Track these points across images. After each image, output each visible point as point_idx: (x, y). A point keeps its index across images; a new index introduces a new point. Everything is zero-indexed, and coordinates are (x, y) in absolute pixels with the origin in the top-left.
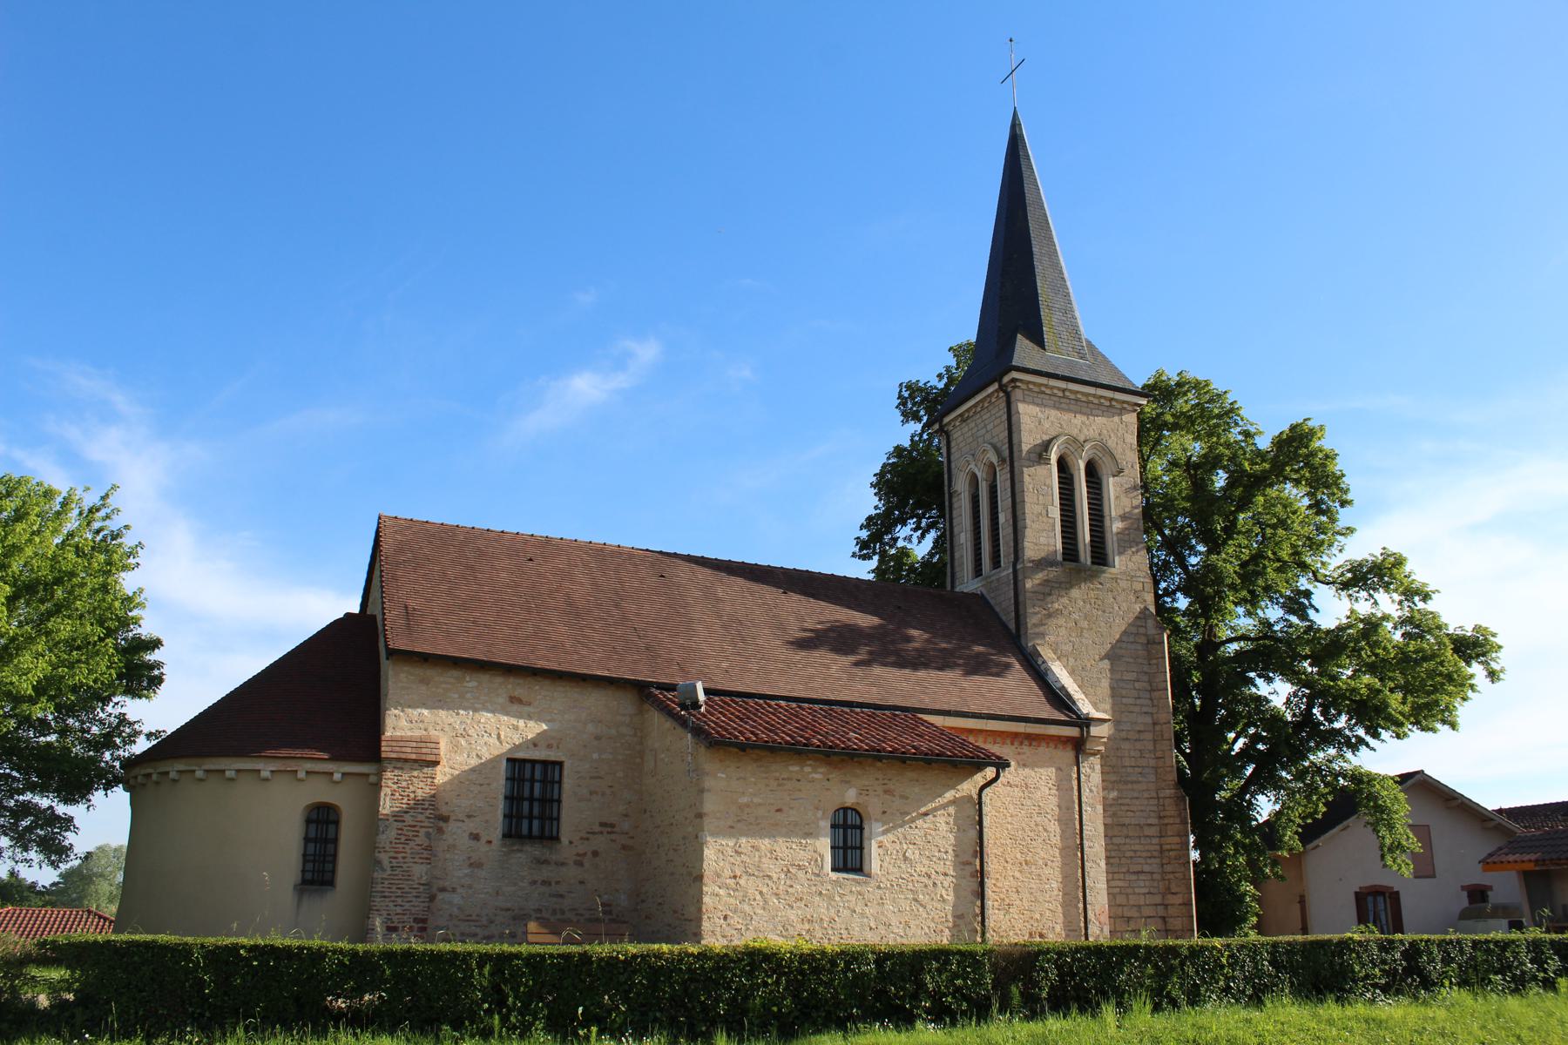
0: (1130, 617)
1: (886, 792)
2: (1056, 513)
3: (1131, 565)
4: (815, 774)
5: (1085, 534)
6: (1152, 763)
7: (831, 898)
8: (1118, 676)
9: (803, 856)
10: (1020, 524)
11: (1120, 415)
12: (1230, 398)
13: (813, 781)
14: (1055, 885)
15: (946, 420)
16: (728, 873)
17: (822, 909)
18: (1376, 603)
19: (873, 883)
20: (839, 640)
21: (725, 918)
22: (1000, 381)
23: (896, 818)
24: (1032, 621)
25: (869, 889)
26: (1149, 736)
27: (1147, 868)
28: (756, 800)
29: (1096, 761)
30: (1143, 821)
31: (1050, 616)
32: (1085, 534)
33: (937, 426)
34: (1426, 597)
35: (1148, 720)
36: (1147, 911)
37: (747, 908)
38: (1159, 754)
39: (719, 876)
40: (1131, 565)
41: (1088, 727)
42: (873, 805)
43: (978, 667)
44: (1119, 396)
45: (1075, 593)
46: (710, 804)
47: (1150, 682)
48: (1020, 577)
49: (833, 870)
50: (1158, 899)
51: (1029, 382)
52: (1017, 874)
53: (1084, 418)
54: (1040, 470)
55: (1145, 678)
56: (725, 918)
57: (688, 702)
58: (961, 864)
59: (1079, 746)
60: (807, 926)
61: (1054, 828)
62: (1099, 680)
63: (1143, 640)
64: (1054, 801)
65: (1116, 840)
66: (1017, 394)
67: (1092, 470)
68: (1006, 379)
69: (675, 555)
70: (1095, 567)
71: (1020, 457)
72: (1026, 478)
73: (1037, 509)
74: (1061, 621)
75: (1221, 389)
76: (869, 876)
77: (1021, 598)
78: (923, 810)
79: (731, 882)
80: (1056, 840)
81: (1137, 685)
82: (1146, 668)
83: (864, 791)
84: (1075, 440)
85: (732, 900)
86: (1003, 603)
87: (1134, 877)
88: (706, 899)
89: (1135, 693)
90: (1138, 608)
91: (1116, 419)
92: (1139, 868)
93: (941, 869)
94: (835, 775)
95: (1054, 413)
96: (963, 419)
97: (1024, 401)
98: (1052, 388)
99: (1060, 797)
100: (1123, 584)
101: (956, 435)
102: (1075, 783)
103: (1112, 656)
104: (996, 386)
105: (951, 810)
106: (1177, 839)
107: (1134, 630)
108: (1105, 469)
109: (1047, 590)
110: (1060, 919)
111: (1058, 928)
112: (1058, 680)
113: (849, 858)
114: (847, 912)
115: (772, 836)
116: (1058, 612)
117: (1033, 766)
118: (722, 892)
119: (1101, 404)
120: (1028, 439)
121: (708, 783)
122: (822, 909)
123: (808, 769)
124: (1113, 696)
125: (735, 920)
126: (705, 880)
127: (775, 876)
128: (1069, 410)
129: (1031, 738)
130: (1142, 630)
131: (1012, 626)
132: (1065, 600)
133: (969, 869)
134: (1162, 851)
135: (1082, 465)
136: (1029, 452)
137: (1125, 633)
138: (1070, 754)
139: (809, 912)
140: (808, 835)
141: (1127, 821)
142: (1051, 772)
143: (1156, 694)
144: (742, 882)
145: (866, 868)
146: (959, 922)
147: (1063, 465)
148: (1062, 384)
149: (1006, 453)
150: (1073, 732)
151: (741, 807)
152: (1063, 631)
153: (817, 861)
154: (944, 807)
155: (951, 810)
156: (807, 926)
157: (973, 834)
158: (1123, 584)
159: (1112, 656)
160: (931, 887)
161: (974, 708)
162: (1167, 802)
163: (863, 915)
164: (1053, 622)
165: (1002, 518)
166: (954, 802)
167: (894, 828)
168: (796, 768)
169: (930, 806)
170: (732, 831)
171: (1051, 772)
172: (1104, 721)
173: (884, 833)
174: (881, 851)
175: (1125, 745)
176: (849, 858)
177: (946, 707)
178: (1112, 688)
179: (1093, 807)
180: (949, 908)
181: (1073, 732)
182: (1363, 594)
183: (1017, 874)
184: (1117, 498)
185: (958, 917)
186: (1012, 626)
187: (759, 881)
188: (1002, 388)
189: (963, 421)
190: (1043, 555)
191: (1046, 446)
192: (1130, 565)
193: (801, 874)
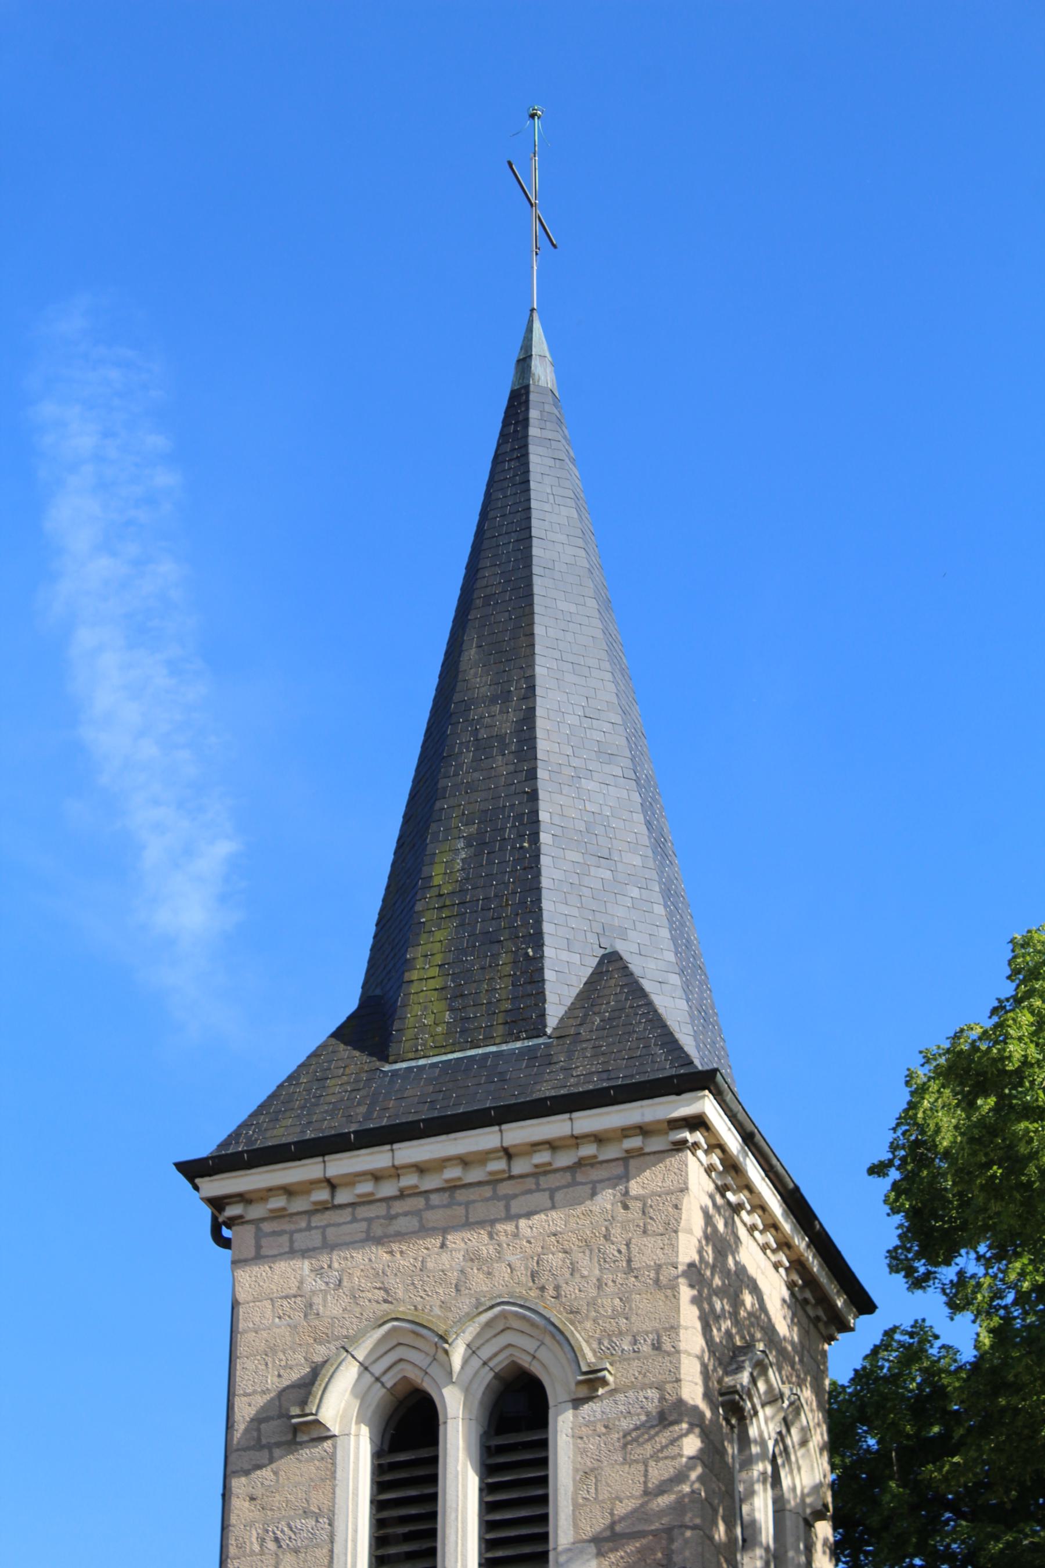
44: (588, 1121)
53: (478, 1240)
54: (296, 1468)
67: (517, 1414)
91: (607, 1199)
95: (360, 1263)
108: (558, 1387)
128: (424, 1230)
136: (258, 1420)
147: (408, 1429)
148: (377, 1158)
184: (587, 1474)
191: (308, 1386)
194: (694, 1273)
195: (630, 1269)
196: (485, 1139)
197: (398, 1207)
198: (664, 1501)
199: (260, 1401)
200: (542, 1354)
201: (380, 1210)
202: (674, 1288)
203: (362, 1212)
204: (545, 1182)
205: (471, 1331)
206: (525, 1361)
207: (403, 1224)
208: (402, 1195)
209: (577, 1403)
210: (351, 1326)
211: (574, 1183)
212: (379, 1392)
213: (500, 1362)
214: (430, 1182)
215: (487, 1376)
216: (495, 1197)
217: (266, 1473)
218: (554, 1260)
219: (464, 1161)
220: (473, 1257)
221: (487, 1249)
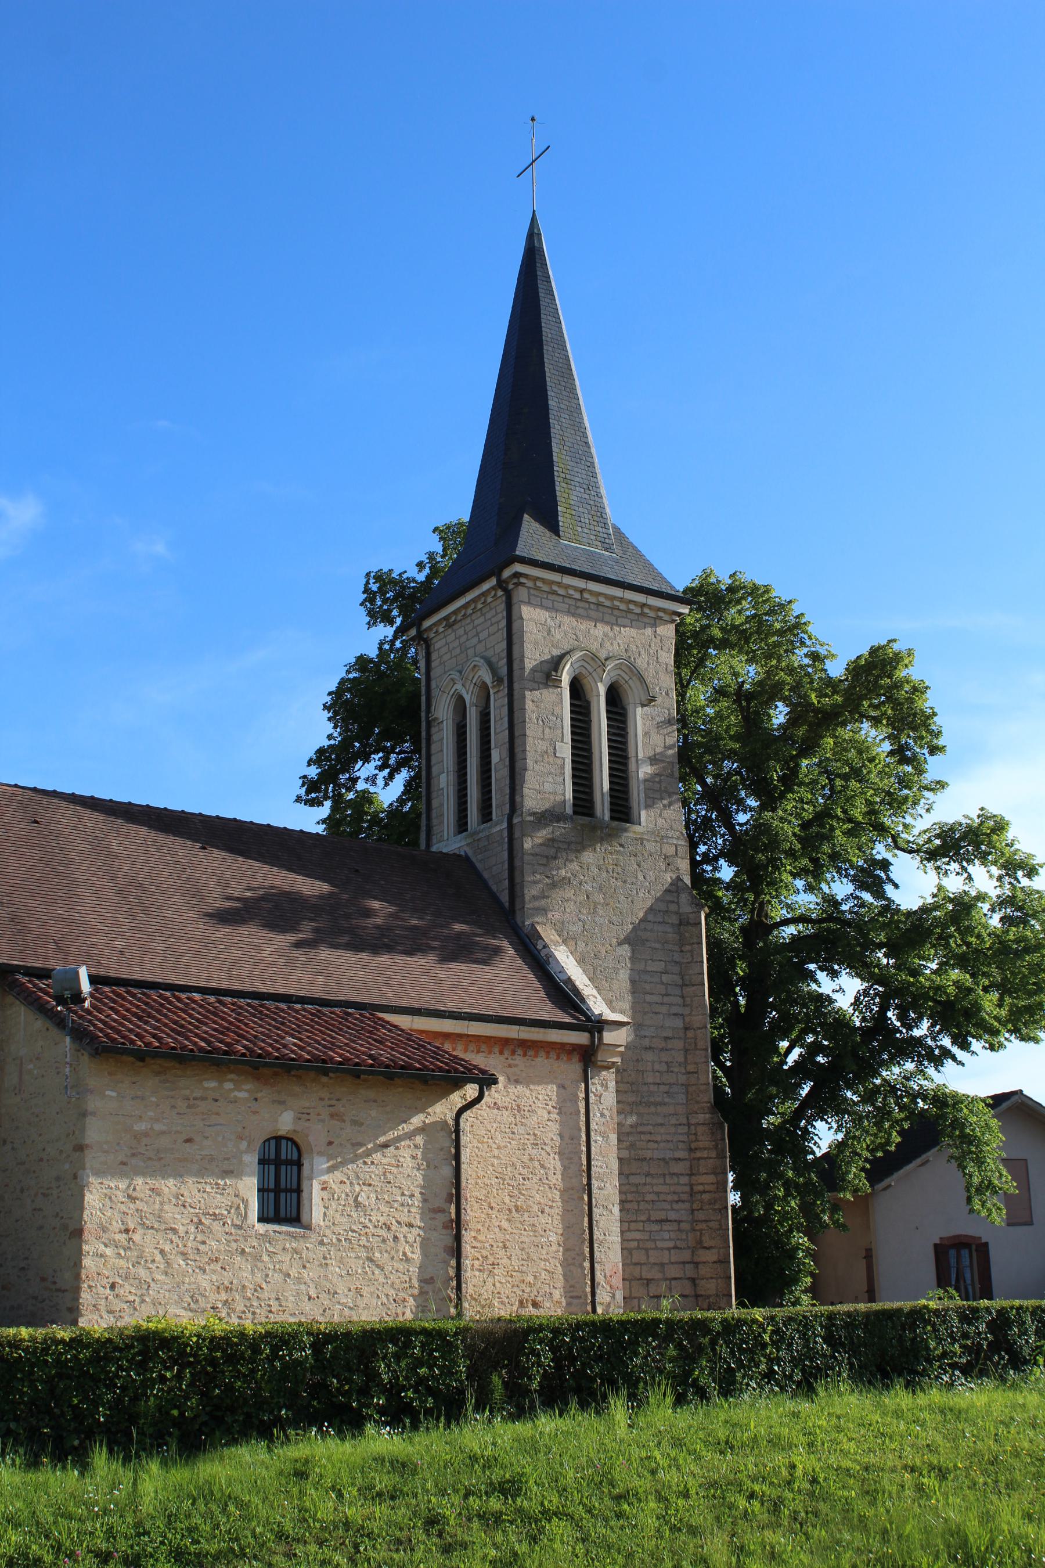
0: (659, 890)
1: (332, 1116)
2: (565, 751)
3: (661, 822)
4: (239, 1090)
6: (682, 1079)
7: (257, 1258)
8: (642, 967)
9: (220, 1202)
10: (518, 765)
11: (654, 625)
12: (796, 609)
13: (235, 1101)
14: (553, 1238)
15: (427, 624)
16: (117, 1226)
17: (244, 1273)
18: (970, 878)
19: (314, 1237)
20: (274, 912)
21: (113, 1287)
22: (499, 575)
23: (347, 1151)
24: (530, 892)
25: (309, 1245)
26: (679, 1044)
27: (672, 1216)
28: (158, 1127)
29: (609, 1077)
30: (669, 1155)
31: (554, 886)
33: (413, 632)
34: (1031, 872)
35: (679, 1023)
36: (673, 1271)
37: (143, 1273)
38: (691, 1068)
39: (104, 1230)
40: (661, 822)
41: (600, 1031)
42: (315, 1134)
43: (458, 951)
45: (588, 856)
46: (95, 1132)
47: (682, 976)
48: (517, 834)
49: (261, 1220)
50: (686, 1255)
51: (538, 578)
52: (505, 1224)
53: (607, 629)
54: (547, 695)
55: (676, 969)
56: (113, 1287)
57: (67, 994)
58: (430, 1211)
59: (588, 1057)
60: (224, 1296)
61: (554, 1163)
62: (616, 971)
63: (674, 919)
64: (555, 1127)
65: (633, 1179)
66: (521, 594)
68: (507, 573)
69: (55, 794)
70: (615, 823)
71: (522, 677)
72: (529, 705)
73: (542, 746)
74: (569, 893)
75: (785, 597)
76: (308, 1227)
77: (517, 863)
78: (382, 1140)
79: (122, 1238)
80: (556, 1179)
81: (665, 978)
82: (677, 957)
83: (303, 1115)
84: (594, 657)
85: (123, 1263)
86: (493, 867)
87: (656, 1227)
88: (87, 1262)
89: (662, 989)
90: (668, 878)
91: (649, 631)
92: (662, 1215)
93: (404, 1219)
94: (265, 1094)
95: (567, 620)
96: (449, 623)
97: (529, 603)
98: (567, 587)
99: (562, 1124)
100: (651, 846)
101: (438, 644)
102: (582, 1105)
103: (634, 940)
104: (493, 581)
105: (419, 1140)
106: (712, 1178)
107: (662, 906)
108: (632, 695)
109: (552, 852)
110: (560, 1282)
111: (557, 1294)
112: (562, 971)
113: (283, 1203)
114: (278, 1277)
115: (178, 1175)
116: (566, 881)
117: (527, 1082)
118: (108, 1251)
119: (629, 611)
120: (533, 655)
121: (93, 1103)
122: (244, 1273)
123: (228, 1085)
124: (633, 993)
125: (126, 1289)
126: (86, 1235)
127: (182, 1230)
128: (588, 618)
129: (526, 1046)
130: (673, 907)
131: (505, 898)
132: (574, 866)
133: (441, 1218)
134: (692, 1193)
135: (602, 690)
136: (533, 670)
137: (651, 910)
138: (574, 1068)
139: (227, 1277)
140: (227, 1173)
141: (649, 1154)
142: (552, 1089)
143: (689, 990)
144: (137, 1237)
145: (304, 1218)
146: (427, 1287)
148: (580, 583)
149: (504, 671)
150: (580, 1038)
151: (137, 1137)
152: (571, 907)
153: (239, 1208)
154: (410, 1136)
155: (419, 1140)
156: (224, 1296)
157: (447, 1171)
158: (651, 846)
159: (634, 940)
160: (391, 1243)
161: (452, 1006)
162: (701, 1129)
163: (299, 1280)
164: (558, 894)
165: (495, 756)
166: (422, 1130)
167: (343, 1164)
168: (213, 1084)
169: (391, 1135)
170: (124, 1168)
171: (552, 1089)
172: (620, 1024)
173: (331, 1170)
174: (325, 1195)
175: (649, 1056)
176: (283, 1203)
177: (415, 1004)
178: (633, 982)
179: (605, 1136)
180: (414, 1270)
181: (580, 1038)
182: (955, 866)
183: (505, 1224)
184: (646, 734)
185: (426, 1281)
186: (505, 898)
187: (159, 1236)
188: (501, 584)
189: (449, 626)
190: (547, 806)
191: (556, 663)
192: (660, 823)
193: (217, 1226)
195: (658, 662)
197: (579, 604)
199: (534, 663)
200: (630, 682)
201: (572, 602)
203: (566, 600)
204: (630, 616)
206: (622, 682)
207: (580, 611)
208: (582, 600)
209: (643, 705)
210: (567, 647)
211: (638, 620)
213: (613, 680)
214: (593, 599)
216: (612, 614)
217: (537, 693)
218: (633, 648)
219: (606, 596)
220: (606, 635)
221: (611, 634)
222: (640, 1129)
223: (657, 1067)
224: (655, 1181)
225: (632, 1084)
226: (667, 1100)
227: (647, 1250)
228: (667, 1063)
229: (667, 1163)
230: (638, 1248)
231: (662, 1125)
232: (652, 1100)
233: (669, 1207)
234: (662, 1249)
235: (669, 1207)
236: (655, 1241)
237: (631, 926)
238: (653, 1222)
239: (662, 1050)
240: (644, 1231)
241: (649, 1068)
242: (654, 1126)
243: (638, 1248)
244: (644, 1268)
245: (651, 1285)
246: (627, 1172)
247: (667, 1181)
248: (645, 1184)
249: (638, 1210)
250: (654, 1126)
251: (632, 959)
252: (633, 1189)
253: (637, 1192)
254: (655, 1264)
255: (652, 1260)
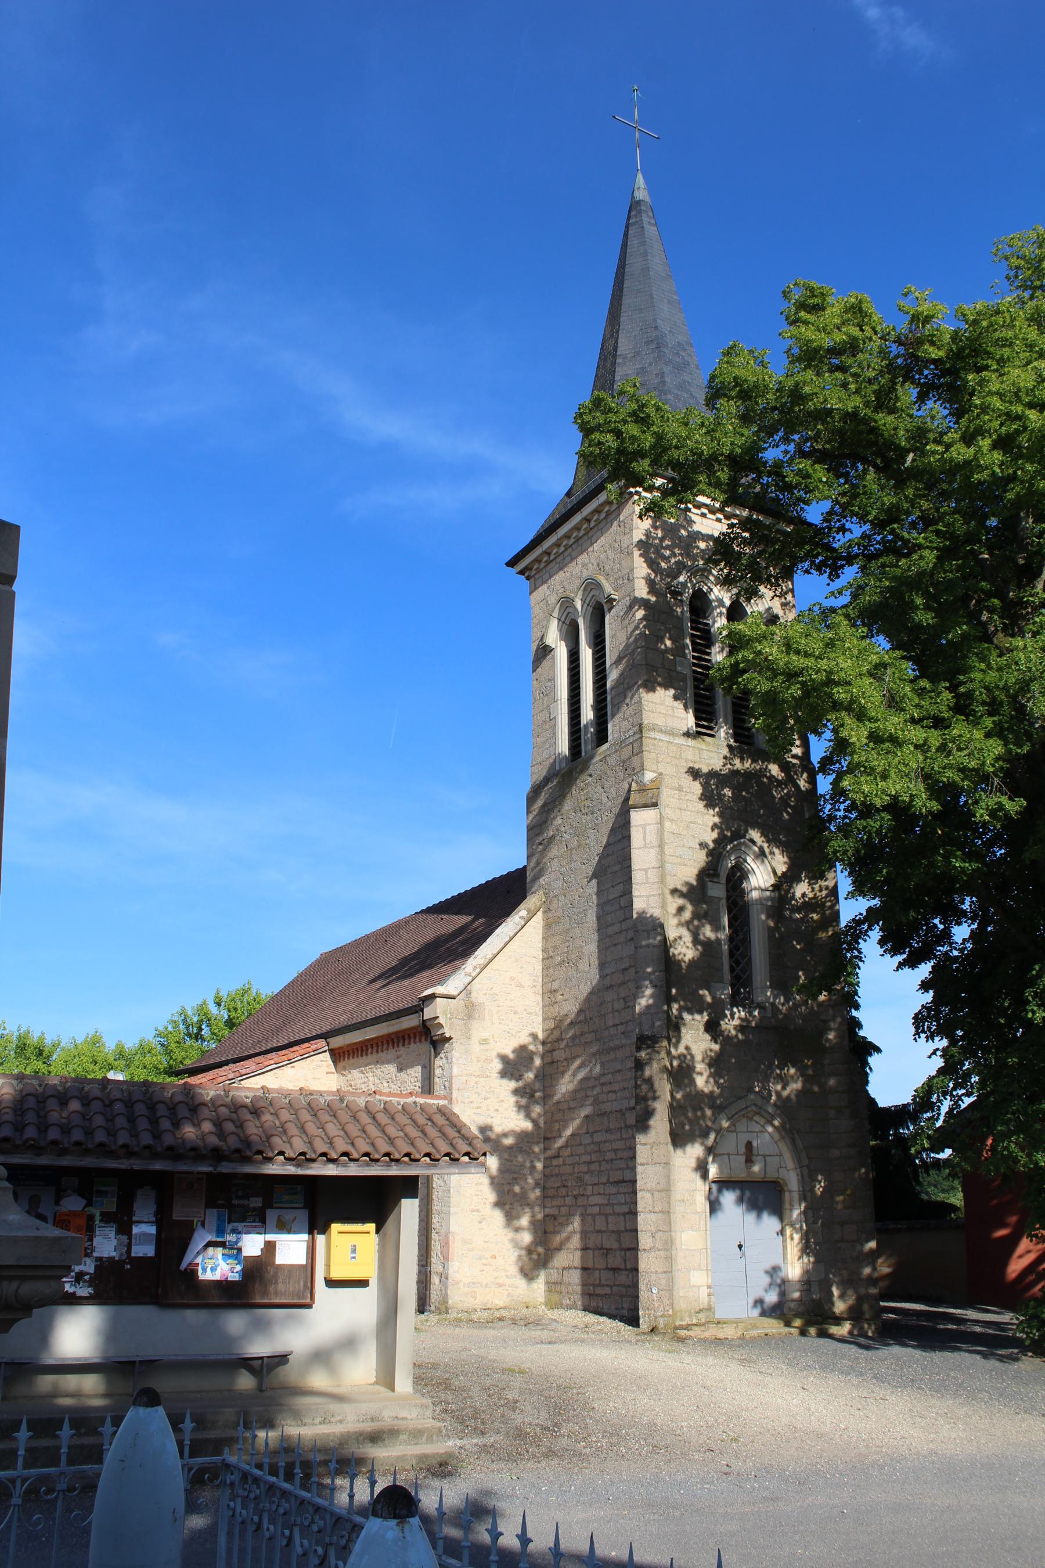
5: (588, 714)
32: (588, 714)
65: (598, 1138)
87: (613, 1190)
116: (552, 839)
137: (612, 829)
178: (598, 918)
184: (613, 637)
194: (640, 544)
196: (577, 518)
198: (632, 639)
202: (630, 554)
205: (580, 593)
212: (565, 627)
215: (590, 609)
222: (602, 1080)
223: (617, 1006)
224: (612, 1137)
225: (595, 1032)
226: (623, 1041)
227: (607, 1215)
228: (624, 999)
229: (624, 1114)
230: (600, 1214)
231: (620, 1071)
232: (612, 1045)
233: (624, 1166)
234: (618, 1214)
235: (624, 1166)
236: (613, 1205)
237: (597, 858)
238: (612, 1183)
239: (620, 985)
240: (604, 1194)
241: (610, 1009)
242: (613, 1073)
243: (600, 1214)
244: (604, 1235)
245: (609, 1256)
246: (591, 1130)
247: (624, 1136)
248: (605, 1142)
249: (599, 1172)
250: (613, 1073)
251: (599, 893)
252: (596, 1149)
253: (599, 1151)
254: (613, 1231)
255: (611, 1227)
